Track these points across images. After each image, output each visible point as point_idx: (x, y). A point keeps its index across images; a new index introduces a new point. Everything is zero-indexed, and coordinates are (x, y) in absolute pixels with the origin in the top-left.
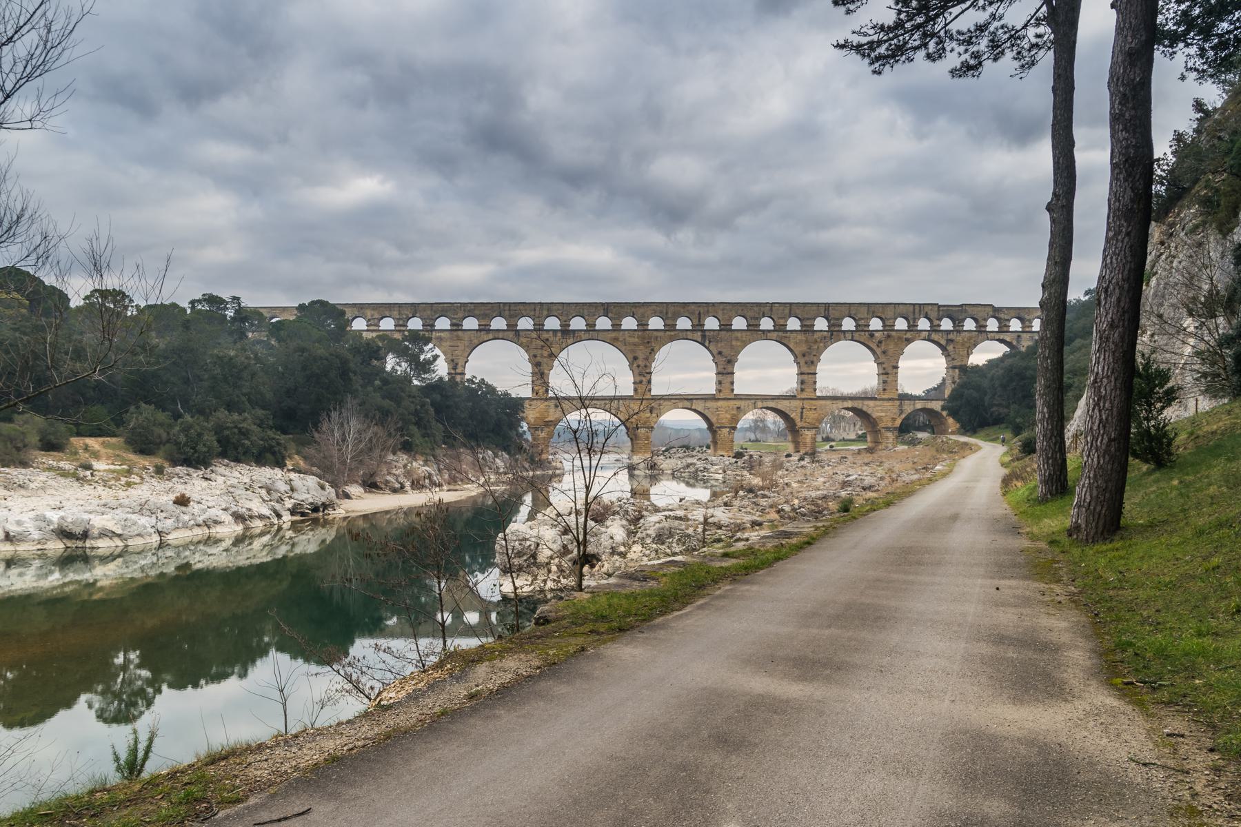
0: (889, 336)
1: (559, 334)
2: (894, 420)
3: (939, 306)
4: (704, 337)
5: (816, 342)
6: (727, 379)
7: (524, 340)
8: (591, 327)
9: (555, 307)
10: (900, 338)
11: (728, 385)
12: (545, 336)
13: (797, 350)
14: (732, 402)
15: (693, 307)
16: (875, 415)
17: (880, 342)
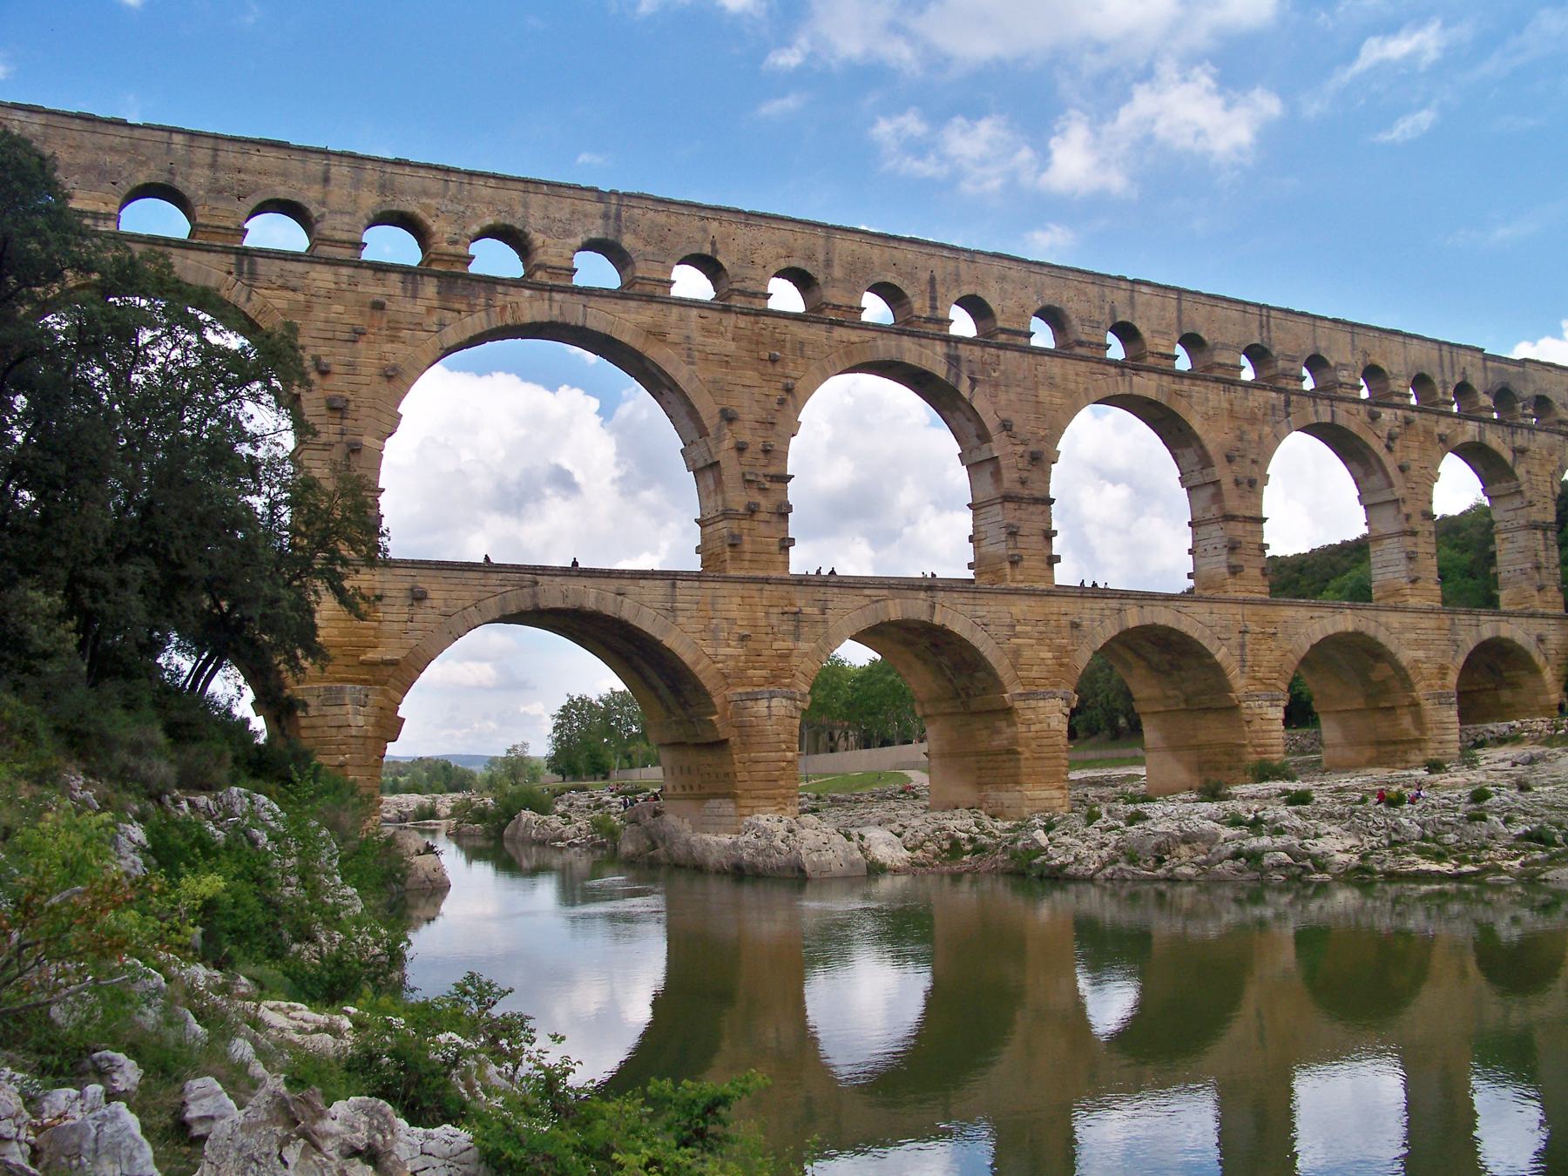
0: (1408, 422)
1: (430, 288)
2: (1443, 671)
3: (1487, 358)
4: (953, 361)
5: (1252, 419)
6: (1027, 519)
7: (280, 300)
8: (546, 278)
9: (405, 178)
10: (1428, 432)
11: (1037, 541)
12: (373, 289)
13: (1214, 437)
14: (1055, 605)
15: (910, 254)
16: (1406, 656)
17: (1391, 438)
